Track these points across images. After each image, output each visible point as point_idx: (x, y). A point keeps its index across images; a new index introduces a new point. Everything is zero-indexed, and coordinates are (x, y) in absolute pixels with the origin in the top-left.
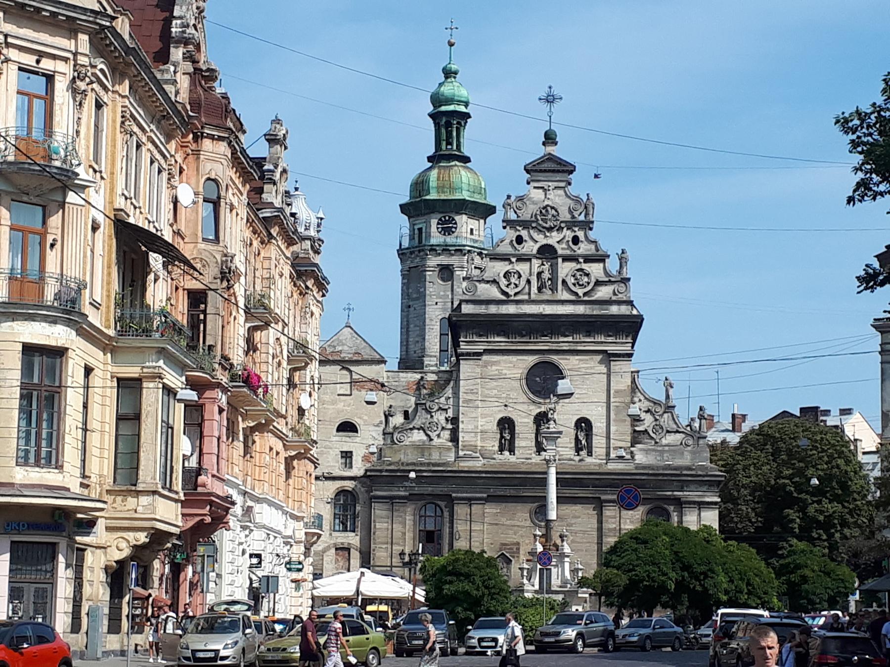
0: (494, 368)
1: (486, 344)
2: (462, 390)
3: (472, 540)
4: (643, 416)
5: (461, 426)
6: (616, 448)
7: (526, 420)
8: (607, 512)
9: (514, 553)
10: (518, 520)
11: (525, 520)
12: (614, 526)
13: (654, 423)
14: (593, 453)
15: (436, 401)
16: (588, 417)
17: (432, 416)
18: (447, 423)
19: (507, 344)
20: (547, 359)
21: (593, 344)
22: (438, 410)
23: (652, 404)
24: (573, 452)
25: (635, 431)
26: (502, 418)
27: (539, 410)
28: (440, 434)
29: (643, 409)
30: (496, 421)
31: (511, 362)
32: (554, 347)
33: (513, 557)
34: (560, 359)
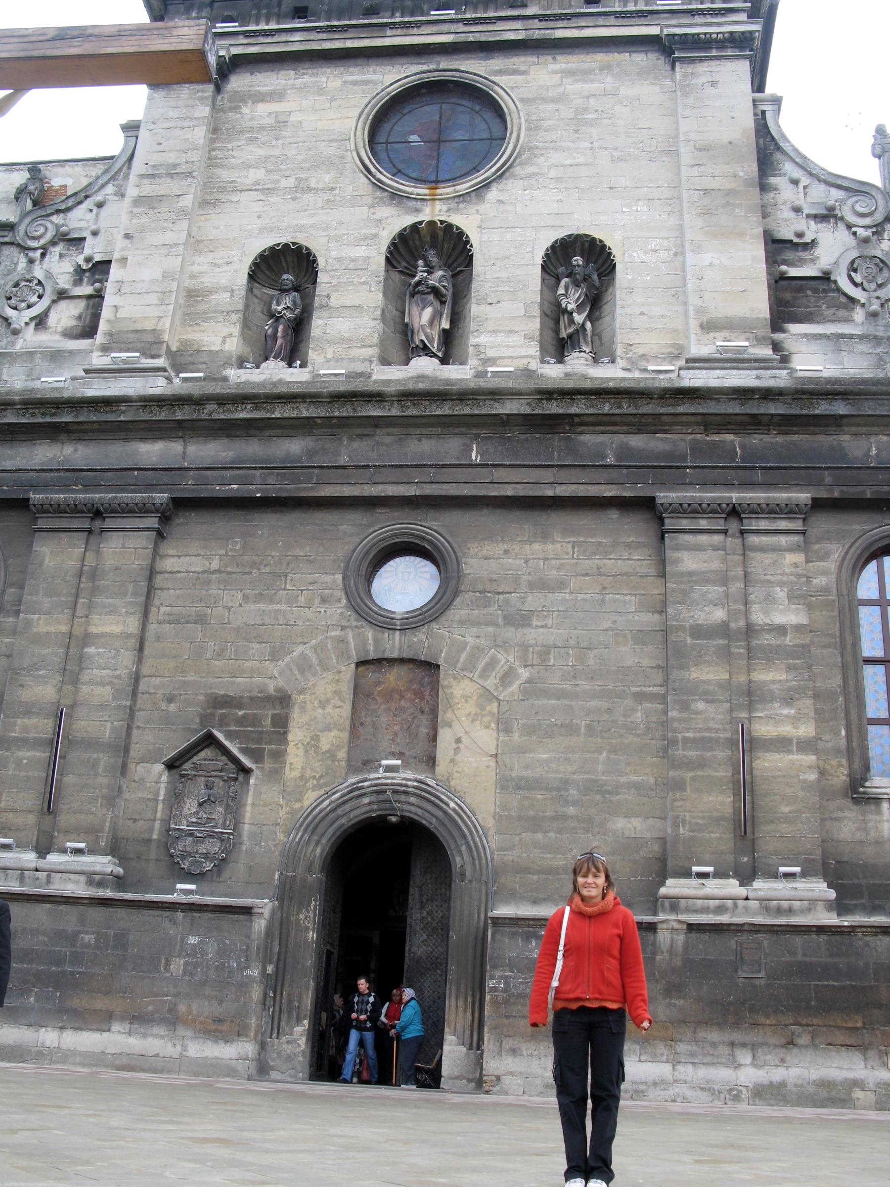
0: (262, 109)
1: (242, 40)
2: (138, 166)
3: (85, 677)
4: (812, 231)
5: (115, 272)
6: (709, 327)
7: (360, 252)
8: (685, 555)
9: (260, 737)
10: (291, 601)
11: (324, 601)
12: (719, 615)
13: (854, 254)
14: (619, 352)
15: (55, 219)
16: (597, 235)
17: (31, 261)
18: (78, 282)
19: (313, 36)
20: (447, 76)
21: (612, 20)
22: (53, 243)
23: (836, 194)
24: (534, 349)
25: (783, 277)
26: (272, 249)
27: (409, 220)
28: (45, 314)
29: (807, 211)
30: (249, 261)
31: (321, 91)
32: (475, 34)
33: (257, 755)
34: (500, 72)
